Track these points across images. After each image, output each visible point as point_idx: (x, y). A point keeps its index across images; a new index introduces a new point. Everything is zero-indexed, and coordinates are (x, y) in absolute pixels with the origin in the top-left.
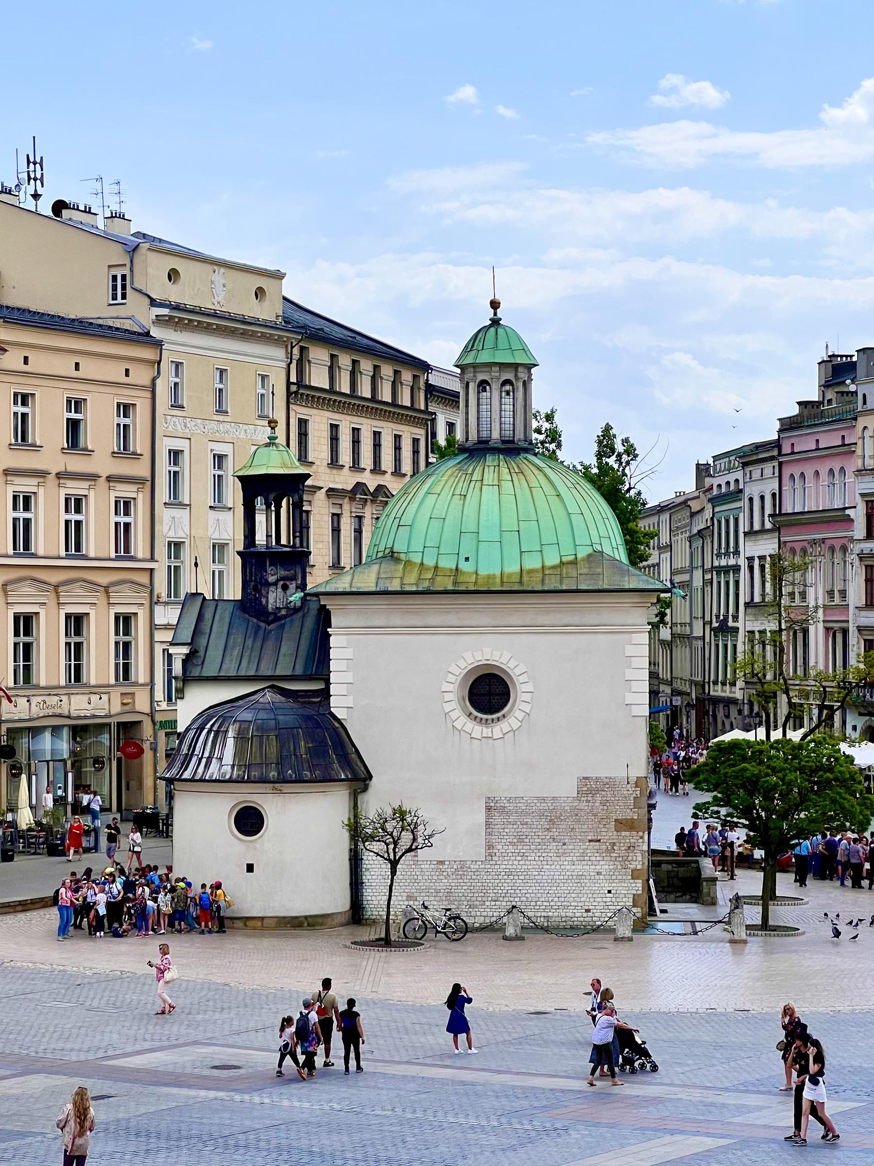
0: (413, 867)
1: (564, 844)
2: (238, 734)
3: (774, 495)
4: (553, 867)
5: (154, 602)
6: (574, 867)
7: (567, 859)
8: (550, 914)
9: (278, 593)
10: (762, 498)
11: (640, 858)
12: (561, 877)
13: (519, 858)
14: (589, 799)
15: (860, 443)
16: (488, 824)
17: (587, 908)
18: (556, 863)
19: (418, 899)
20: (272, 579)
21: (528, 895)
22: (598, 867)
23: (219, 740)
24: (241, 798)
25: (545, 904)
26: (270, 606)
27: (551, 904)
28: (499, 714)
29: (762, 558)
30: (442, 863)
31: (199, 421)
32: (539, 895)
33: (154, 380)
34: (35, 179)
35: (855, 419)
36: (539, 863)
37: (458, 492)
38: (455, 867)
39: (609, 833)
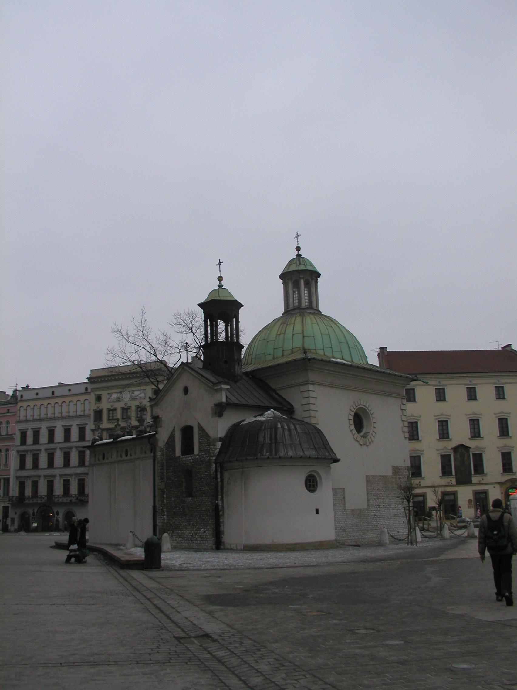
1: (390, 499)
6: (393, 511)
7: (392, 506)
15: (18, 412)
17: (398, 531)
19: (347, 530)
30: (353, 510)
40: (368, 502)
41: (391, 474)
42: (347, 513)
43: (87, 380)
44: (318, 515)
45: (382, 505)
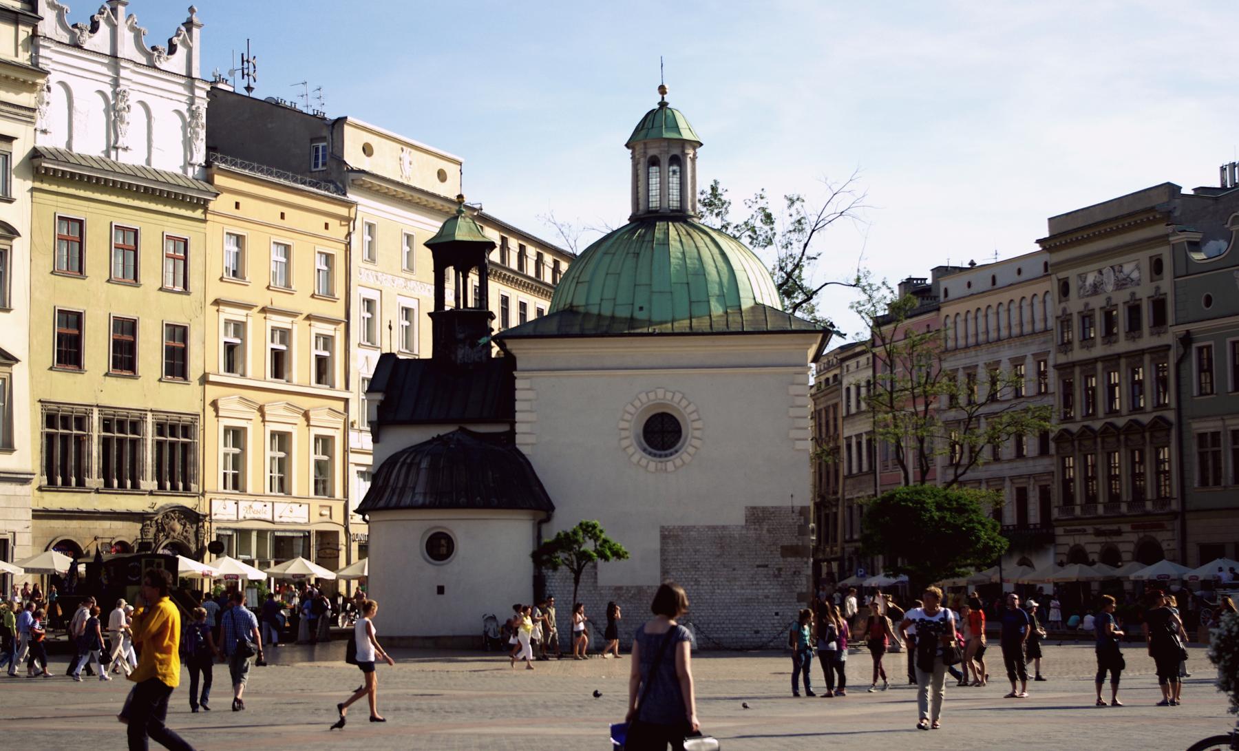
0: (593, 592)
1: (734, 569)
3: (868, 382)
4: (724, 591)
5: (348, 426)
6: (743, 591)
8: (722, 636)
10: (858, 387)
11: (804, 582)
12: (732, 601)
13: (692, 583)
14: (757, 527)
16: (663, 551)
17: (755, 629)
18: (726, 587)
20: (461, 336)
21: (701, 618)
22: (766, 591)
24: (433, 524)
25: (718, 626)
26: (459, 361)
27: (723, 626)
28: (672, 450)
29: (859, 436)
30: (620, 588)
31: (389, 276)
32: (711, 618)
33: (349, 234)
34: (248, 75)
35: (938, 309)
36: (711, 587)
37: (632, 251)
39: (777, 560)
40: (664, 575)
41: (743, 523)
42: (601, 594)
43: (1038, 245)
44: (441, 596)
45: (705, 580)
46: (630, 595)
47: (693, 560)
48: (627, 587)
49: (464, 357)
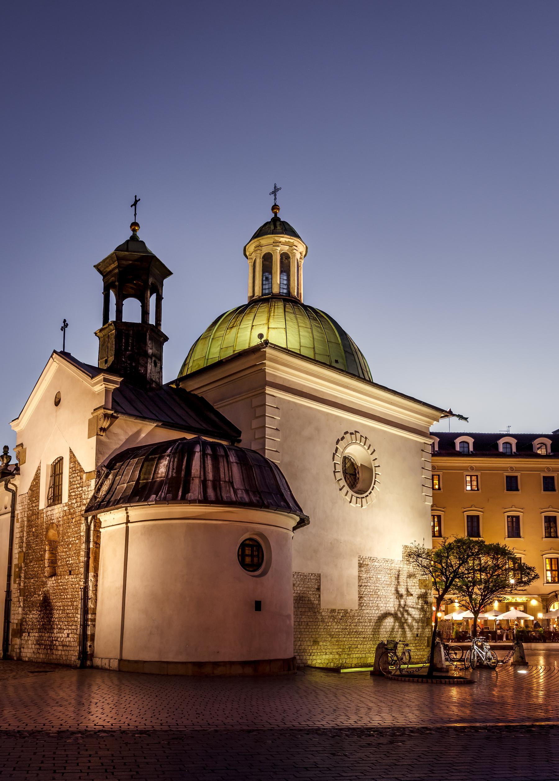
2: (239, 460)
9: (153, 367)
23: (221, 465)
26: (148, 376)
30: (333, 611)
38: (341, 615)
40: (360, 600)
46: (340, 617)
47: (376, 588)
48: (338, 610)
49: (151, 373)
